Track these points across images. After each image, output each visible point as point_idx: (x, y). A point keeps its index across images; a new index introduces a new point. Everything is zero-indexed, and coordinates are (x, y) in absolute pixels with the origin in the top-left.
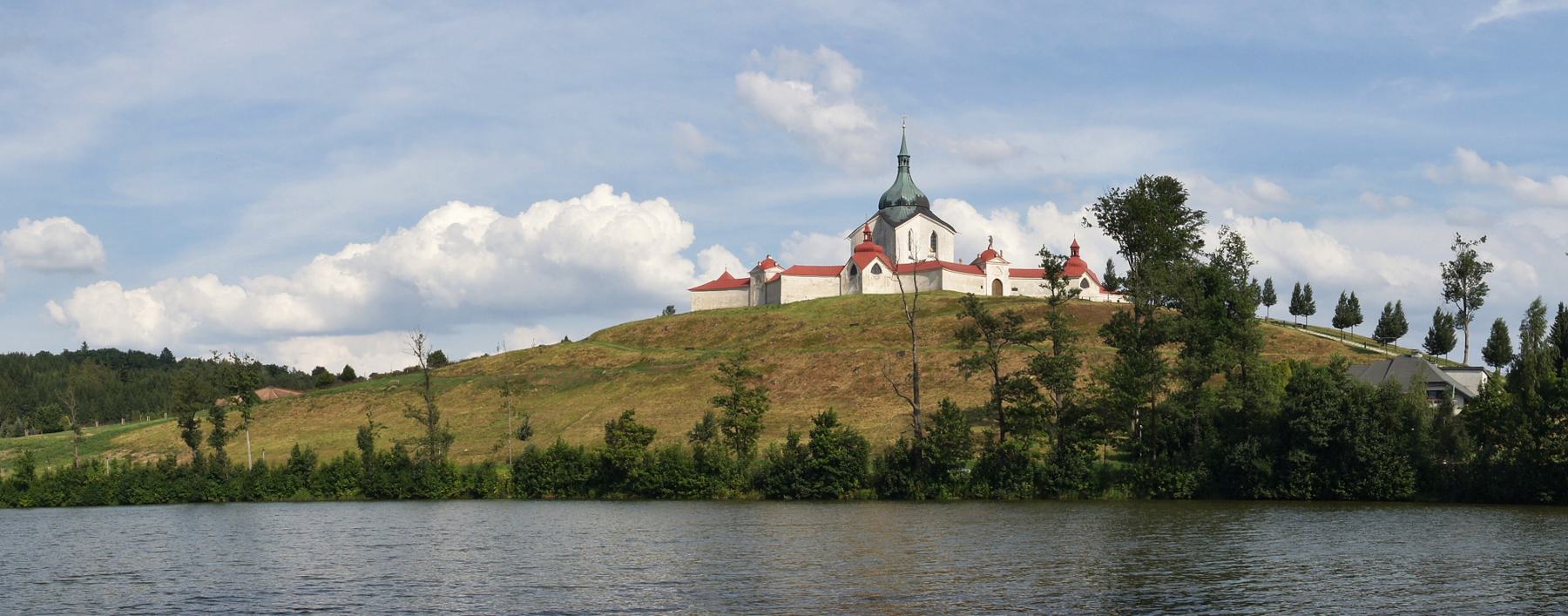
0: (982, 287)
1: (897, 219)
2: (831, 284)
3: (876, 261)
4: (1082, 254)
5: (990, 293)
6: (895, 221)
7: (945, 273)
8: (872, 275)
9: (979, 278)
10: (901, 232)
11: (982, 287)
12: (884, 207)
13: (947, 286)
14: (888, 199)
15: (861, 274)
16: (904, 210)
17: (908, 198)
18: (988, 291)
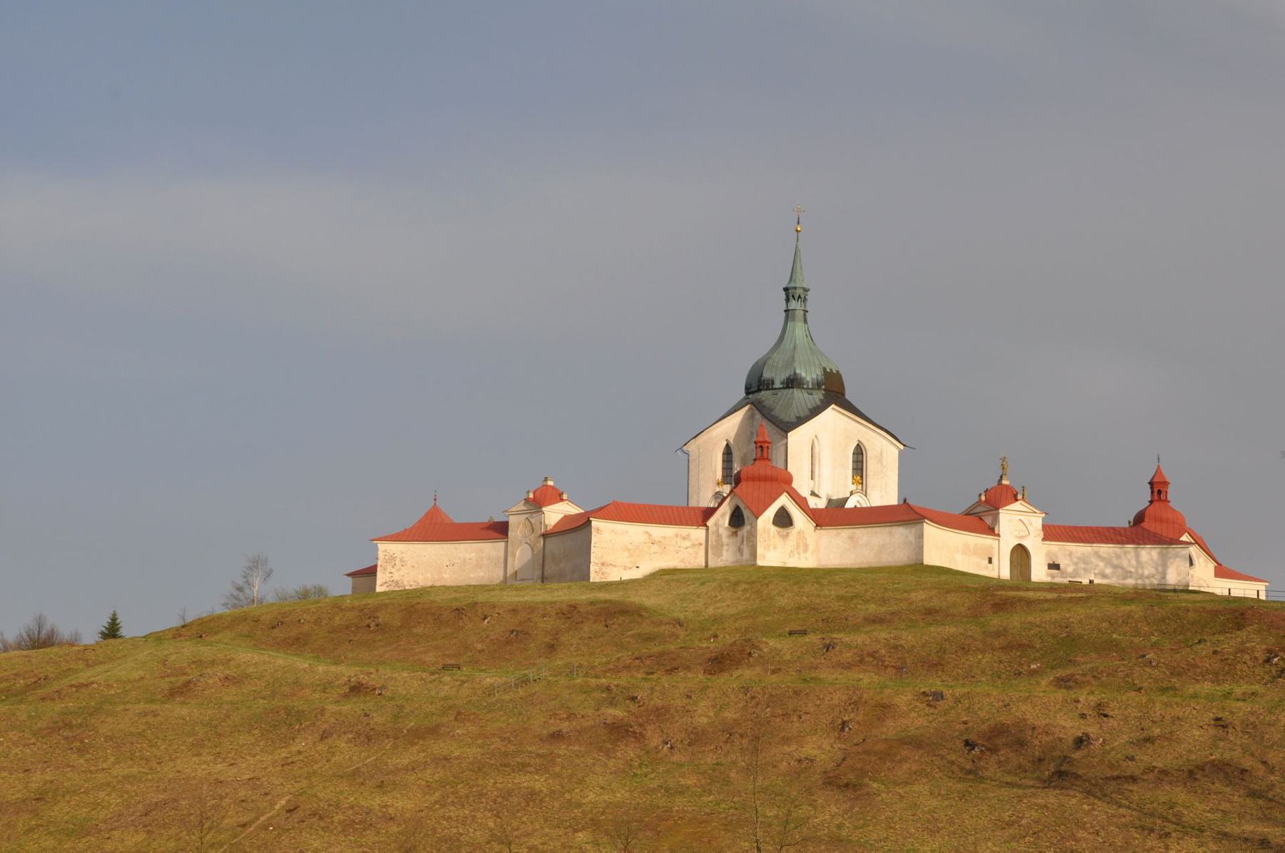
0: (990, 561)
2: (688, 543)
3: (784, 500)
4: (1174, 496)
5: (1005, 574)
6: (787, 419)
7: (930, 530)
8: (774, 529)
9: (986, 540)
10: (798, 439)
11: (990, 561)
12: (759, 390)
13: (932, 557)
14: (767, 375)
15: (754, 526)
16: (801, 399)
18: (1002, 570)
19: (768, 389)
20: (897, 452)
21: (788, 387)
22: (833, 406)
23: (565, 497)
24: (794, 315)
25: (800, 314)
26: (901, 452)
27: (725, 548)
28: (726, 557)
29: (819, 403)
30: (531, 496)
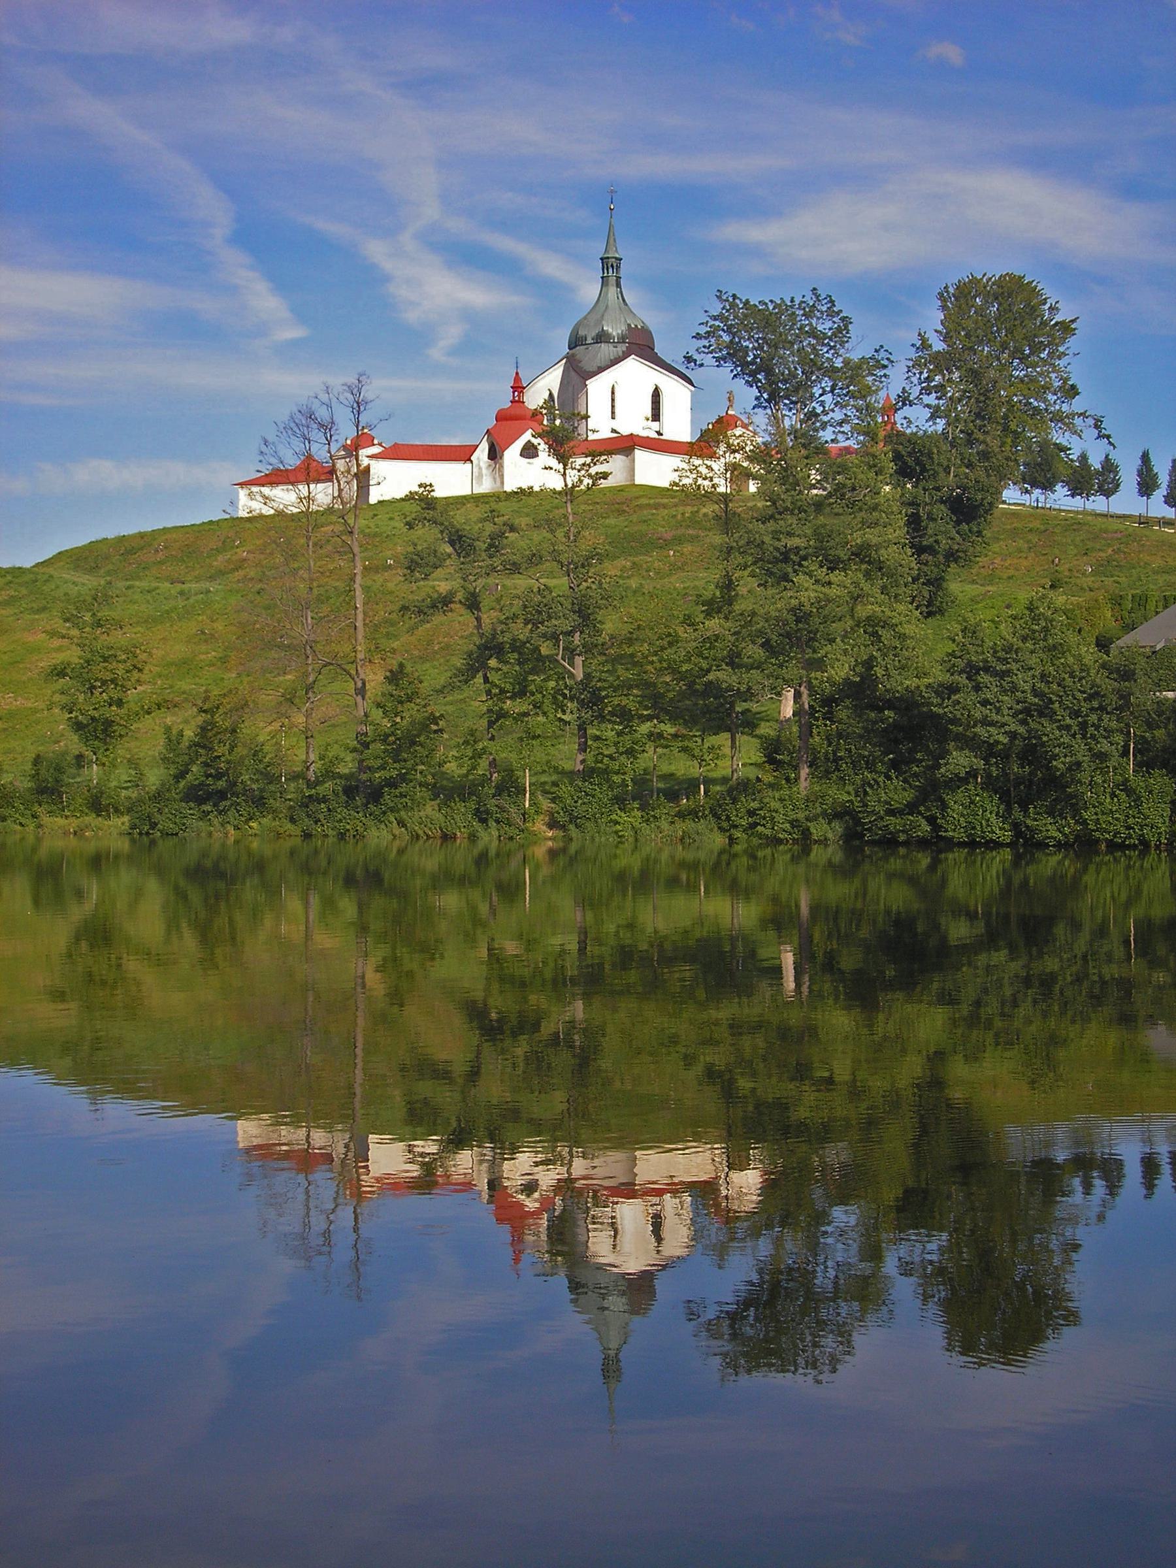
1: (592, 367)
3: (527, 436)
7: (640, 455)
10: (598, 388)
14: (582, 333)
16: (606, 351)
17: (614, 329)
19: (582, 345)
20: (689, 394)
21: (597, 343)
22: (633, 356)
23: (376, 442)
24: (607, 281)
25: (613, 280)
26: (693, 395)
27: (484, 478)
28: (486, 486)
29: (620, 354)
30: (349, 442)
